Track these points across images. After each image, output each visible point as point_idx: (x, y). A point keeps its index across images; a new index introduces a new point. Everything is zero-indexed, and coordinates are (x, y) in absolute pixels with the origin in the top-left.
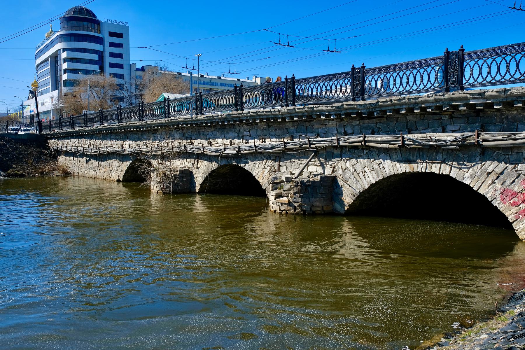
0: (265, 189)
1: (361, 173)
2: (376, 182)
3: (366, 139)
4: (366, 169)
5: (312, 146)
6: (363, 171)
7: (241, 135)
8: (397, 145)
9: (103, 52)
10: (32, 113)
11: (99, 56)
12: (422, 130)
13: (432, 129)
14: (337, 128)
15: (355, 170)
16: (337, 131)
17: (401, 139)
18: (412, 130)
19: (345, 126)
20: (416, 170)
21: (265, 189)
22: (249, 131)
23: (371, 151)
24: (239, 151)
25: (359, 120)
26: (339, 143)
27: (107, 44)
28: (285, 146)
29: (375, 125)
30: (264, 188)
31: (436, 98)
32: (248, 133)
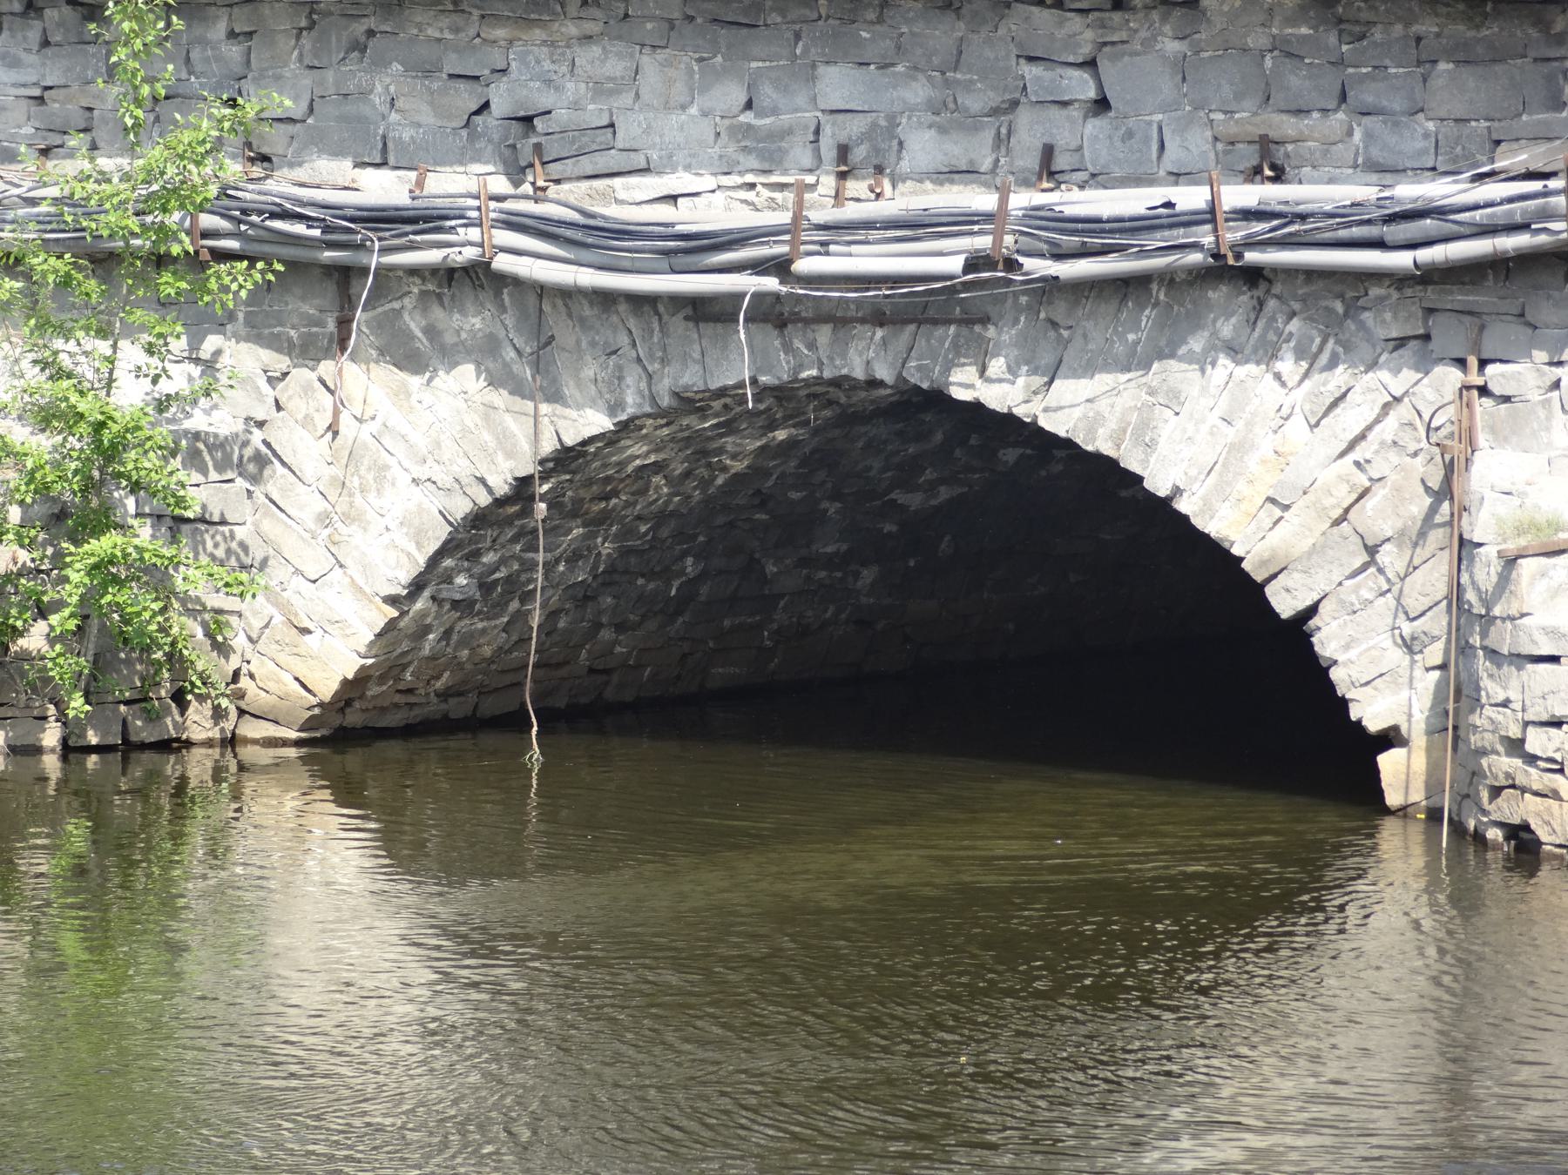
0: (1312, 610)
21: (1312, 610)
22: (1090, 64)
30: (1285, 602)
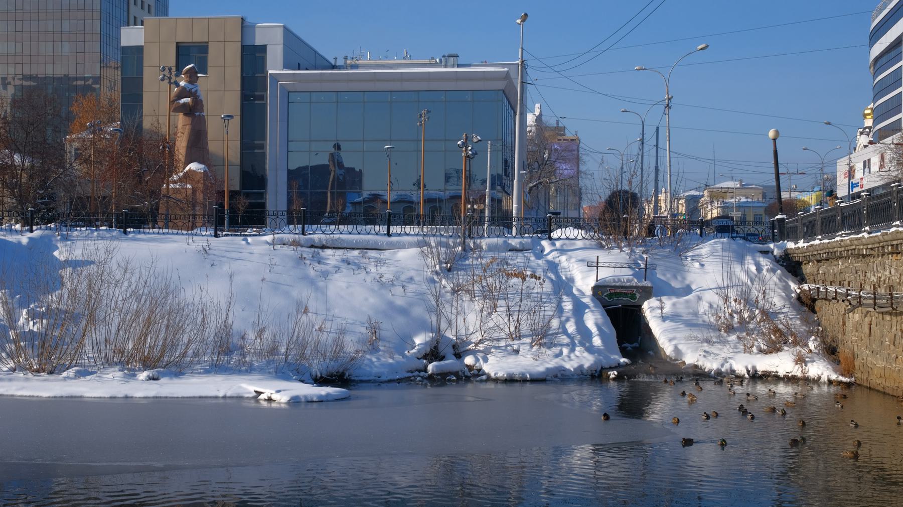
10: (856, 190)
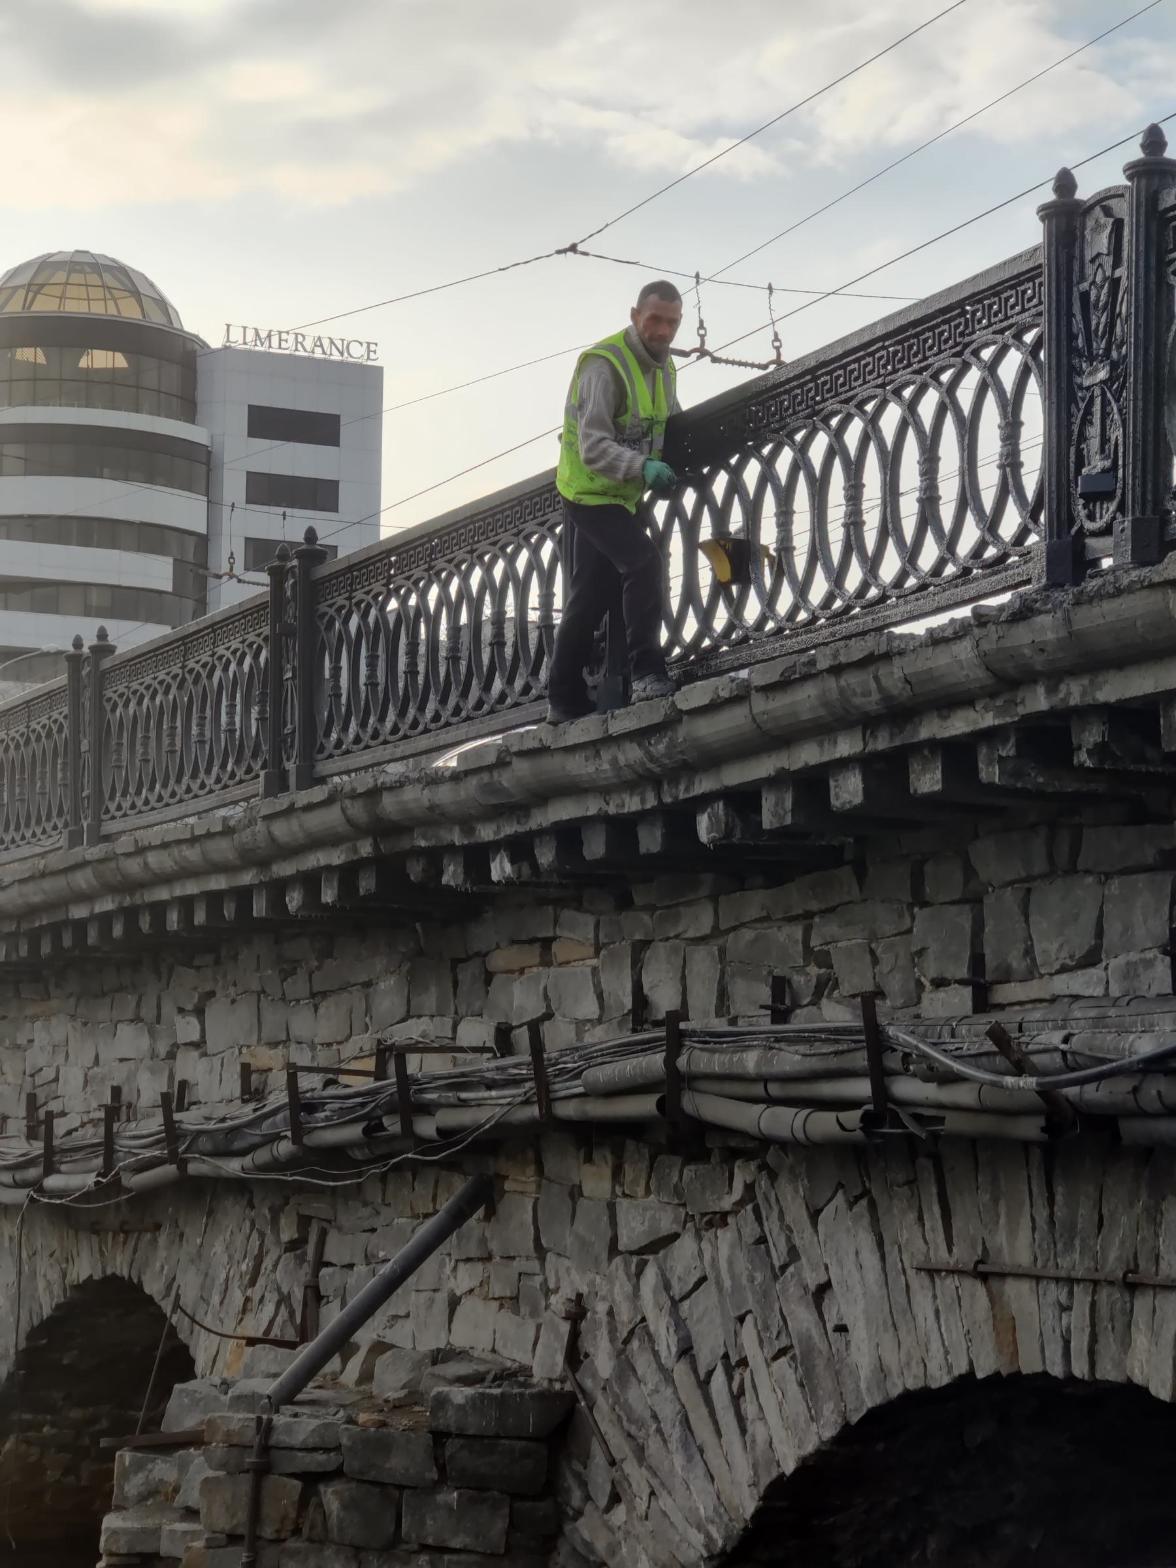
1: (719, 1378)
2: (806, 1467)
3: (682, 1062)
4: (748, 1333)
5: (426, 1127)
6: (734, 1360)
7: (162, 1049)
8: (852, 1118)
9: (203, 542)
11: (178, 564)
12: (1063, 969)
13: (1121, 960)
14: (595, 970)
15: (686, 1351)
16: (600, 996)
17: (861, 1060)
18: (1006, 977)
19: (640, 949)
20: (1029, 1364)
22: (200, 1012)
23: (773, 1176)
24: (109, 1164)
25: (714, 899)
26: (545, 1095)
27: (233, 487)
28: (298, 1131)
29: (798, 932)
31: (985, 646)
32: (188, 1029)
